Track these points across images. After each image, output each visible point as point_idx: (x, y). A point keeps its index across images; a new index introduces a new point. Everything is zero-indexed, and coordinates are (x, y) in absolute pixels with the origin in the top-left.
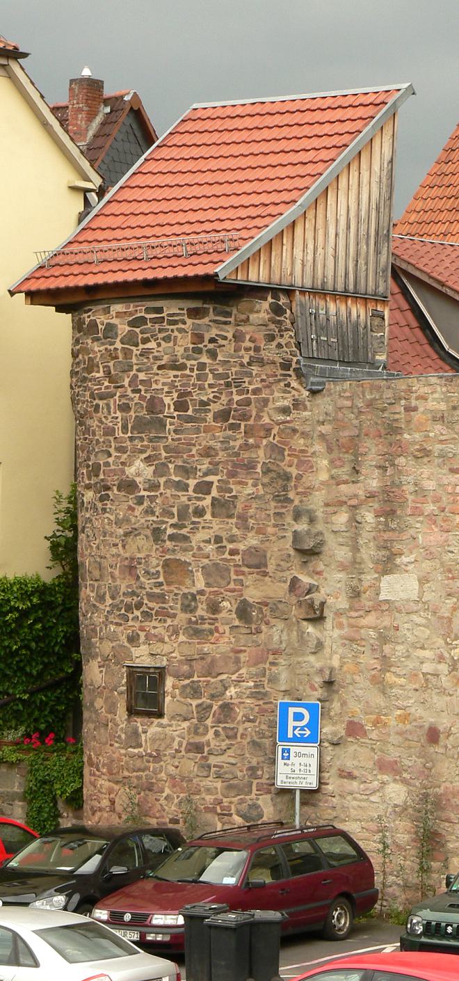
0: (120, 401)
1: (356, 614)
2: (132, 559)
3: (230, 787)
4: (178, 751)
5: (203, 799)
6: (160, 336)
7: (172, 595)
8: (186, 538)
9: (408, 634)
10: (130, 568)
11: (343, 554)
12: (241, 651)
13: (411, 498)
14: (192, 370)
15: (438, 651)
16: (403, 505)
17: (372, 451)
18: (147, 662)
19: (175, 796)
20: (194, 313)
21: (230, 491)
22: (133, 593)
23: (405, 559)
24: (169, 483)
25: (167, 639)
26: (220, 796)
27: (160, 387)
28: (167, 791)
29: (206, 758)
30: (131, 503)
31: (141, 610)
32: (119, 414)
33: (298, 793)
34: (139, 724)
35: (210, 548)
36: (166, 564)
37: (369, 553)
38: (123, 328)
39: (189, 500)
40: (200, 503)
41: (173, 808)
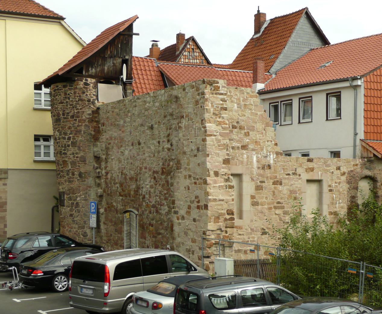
3: (79, 227)
12: (80, 187)
21: (75, 139)
26: (77, 230)
29: (73, 218)
40: (69, 143)
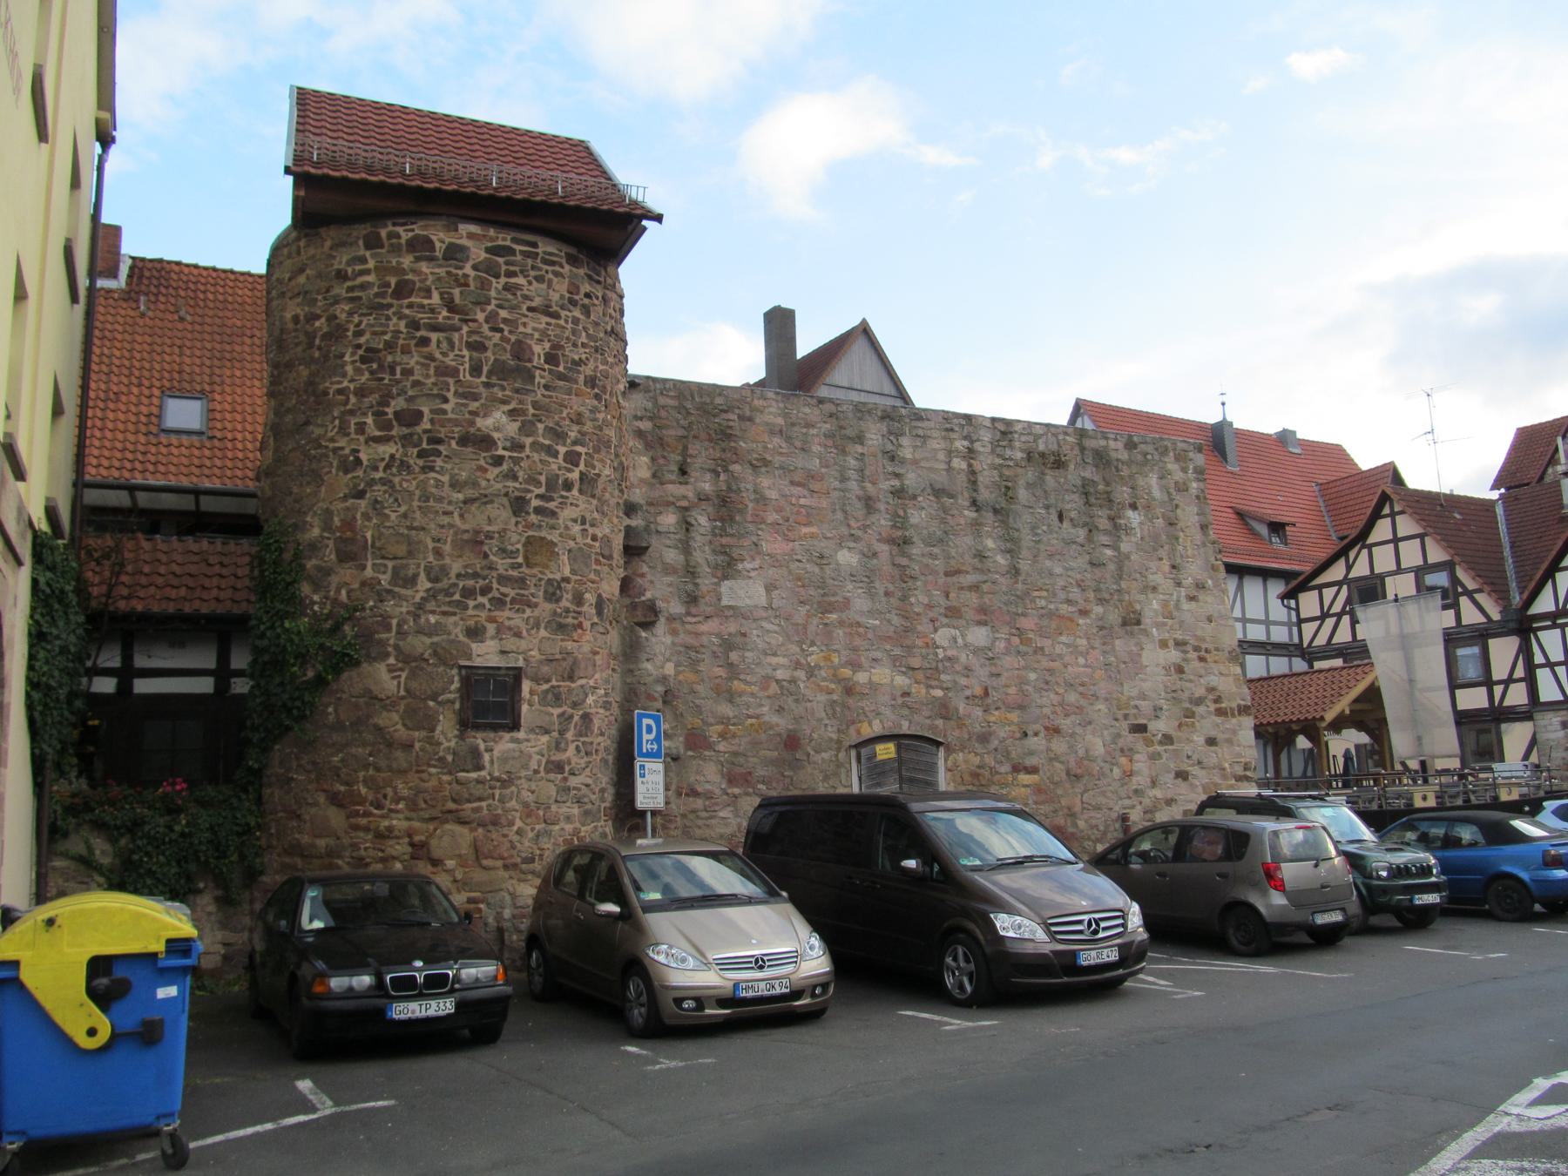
0: (468, 337)
1: (694, 620)
2: (477, 532)
3: (587, 813)
4: (536, 772)
5: (562, 829)
6: (532, 273)
7: (534, 580)
8: (553, 514)
9: (758, 641)
10: (475, 542)
11: (672, 556)
12: (598, 653)
13: (751, 505)
14: (566, 322)
15: (794, 658)
16: (742, 512)
17: (702, 455)
18: (494, 661)
19: (529, 828)
20: (573, 261)
21: (594, 467)
22: (476, 575)
23: (748, 566)
24: (536, 446)
25: (524, 633)
26: (577, 825)
27: (529, 331)
28: (518, 823)
29: (565, 779)
30: (482, 462)
31: (490, 596)
32: (465, 352)
33: (649, 814)
34: (480, 741)
35: (577, 528)
36: (529, 542)
37: (702, 556)
38: (478, 253)
39: (560, 469)
40: (570, 475)
41: (527, 844)
